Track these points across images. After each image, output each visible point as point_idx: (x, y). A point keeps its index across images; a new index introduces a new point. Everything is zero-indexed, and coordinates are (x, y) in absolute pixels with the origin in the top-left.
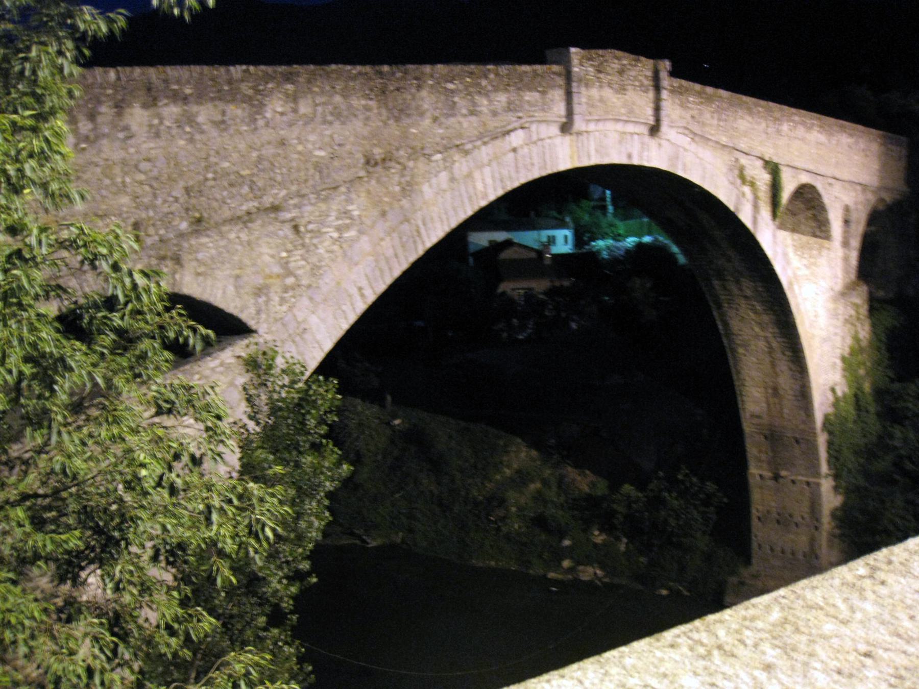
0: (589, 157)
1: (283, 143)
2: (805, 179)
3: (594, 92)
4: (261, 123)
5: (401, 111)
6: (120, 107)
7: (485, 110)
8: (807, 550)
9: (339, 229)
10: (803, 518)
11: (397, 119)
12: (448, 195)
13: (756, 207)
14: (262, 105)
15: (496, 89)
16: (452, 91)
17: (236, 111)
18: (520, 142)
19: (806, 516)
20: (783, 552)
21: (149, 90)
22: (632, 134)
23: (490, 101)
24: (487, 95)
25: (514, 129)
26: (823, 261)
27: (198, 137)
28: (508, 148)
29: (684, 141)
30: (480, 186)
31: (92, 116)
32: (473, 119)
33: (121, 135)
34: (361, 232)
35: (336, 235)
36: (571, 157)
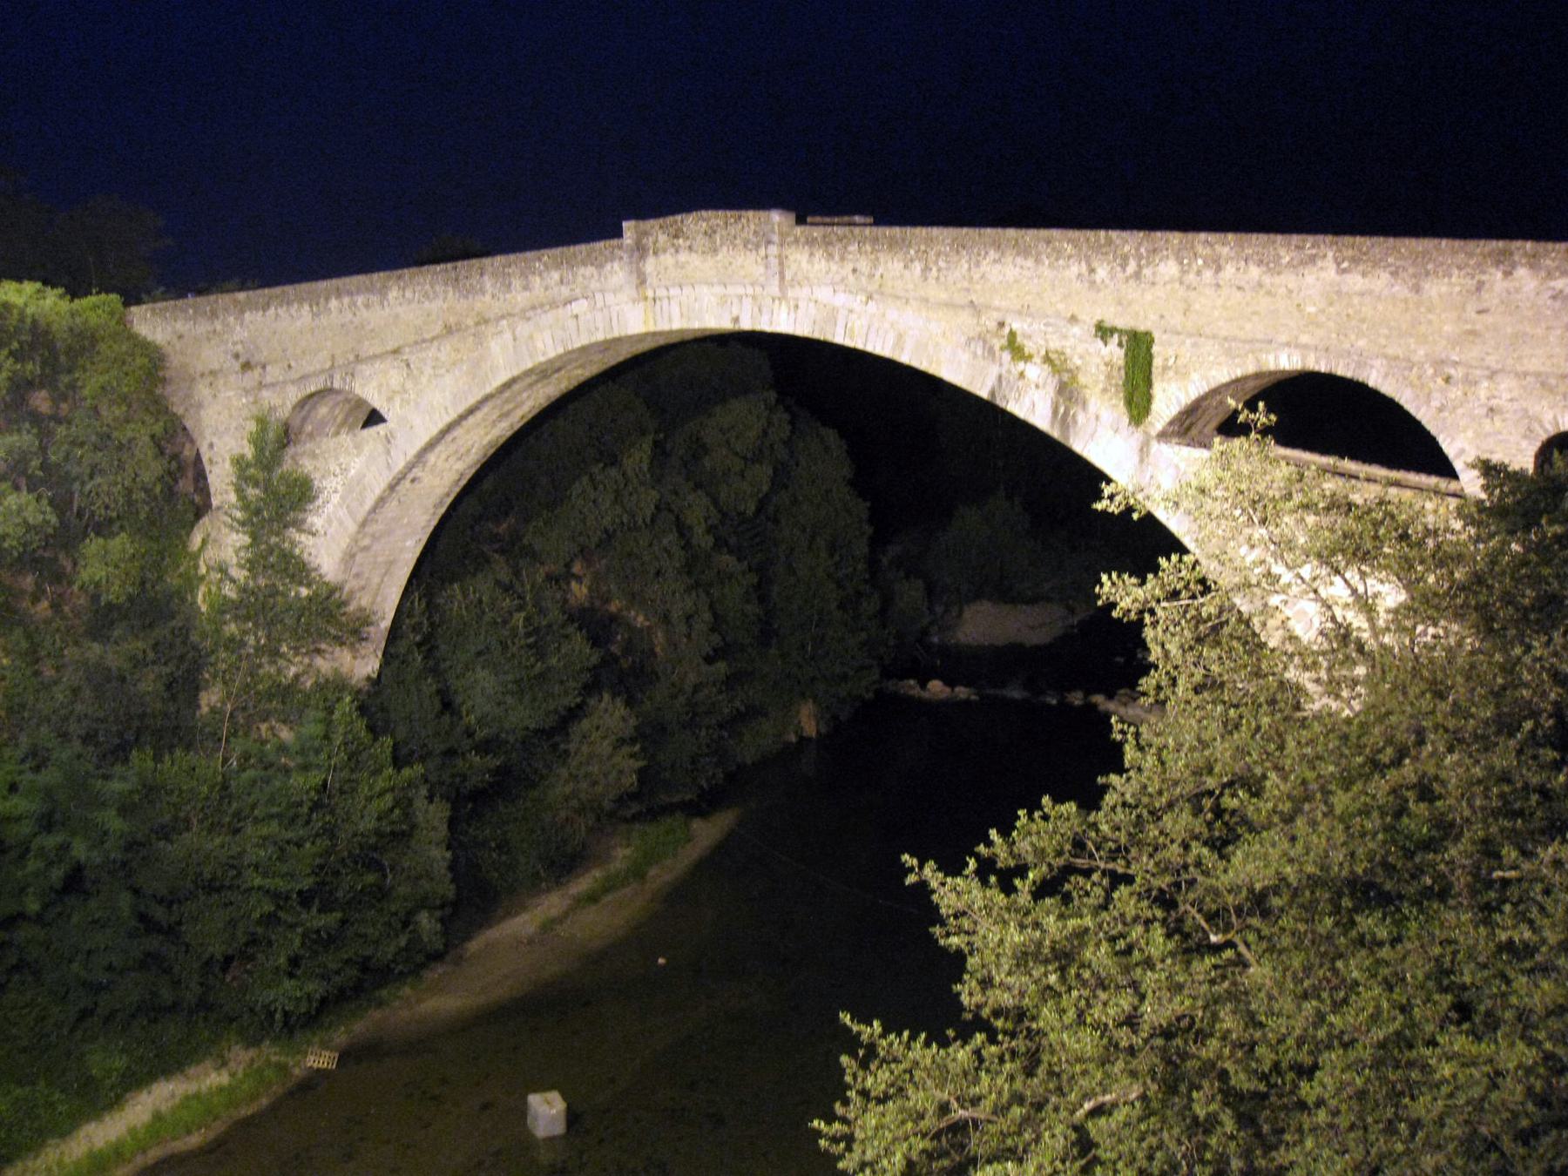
0: (670, 320)
3: (667, 259)
6: (327, 299)
9: (434, 368)
14: (386, 294)
17: (374, 298)
22: (740, 298)
24: (540, 275)
30: (540, 345)
31: (317, 304)
32: (527, 294)
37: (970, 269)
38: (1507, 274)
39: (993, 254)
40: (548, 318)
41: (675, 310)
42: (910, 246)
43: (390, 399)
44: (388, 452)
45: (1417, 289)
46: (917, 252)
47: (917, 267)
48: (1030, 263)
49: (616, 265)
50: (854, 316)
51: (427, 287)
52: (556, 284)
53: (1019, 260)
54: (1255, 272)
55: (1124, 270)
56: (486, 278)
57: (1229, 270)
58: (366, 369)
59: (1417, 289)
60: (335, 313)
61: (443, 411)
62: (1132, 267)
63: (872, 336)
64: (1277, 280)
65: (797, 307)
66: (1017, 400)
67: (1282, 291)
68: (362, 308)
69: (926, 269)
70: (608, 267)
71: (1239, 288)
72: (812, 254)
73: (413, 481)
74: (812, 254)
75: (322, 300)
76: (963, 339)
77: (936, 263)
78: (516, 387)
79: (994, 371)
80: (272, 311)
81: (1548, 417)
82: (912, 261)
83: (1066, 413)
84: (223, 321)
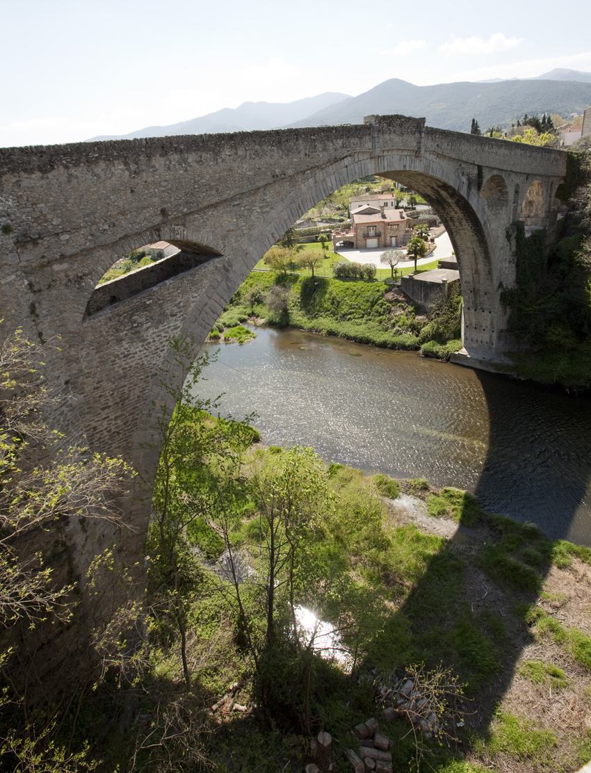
1: (230, 170)
2: (495, 172)
3: (387, 136)
4: (220, 160)
5: (289, 151)
6: (149, 157)
7: (331, 148)
8: (488, 340)
9: (261, 208)
10: (487, 327)
11: (287, 155)
12: (314, 189)
13: (469, 188)
15: (336, 138)
16: (314, 140)
17: (206, 156)
19: (489, 326)
20: (477, 341)
21: (163, 147)
23: (334, 144)
25: (346, 157)
26: (503, 212)
27: (188, 168)
28: (343, 166)
29: (432, 157)
30: (329, 184)
33: (151, 170)
34: (272, 208)
35: (259, 210)
36: (375, 169)
40: (331, 169)
47: (450, 144)
49: (367, 137)
52: (341, 148)
56: (300, 141)
60: (161, 170)
61: (270, 236)
68: (194, 164)
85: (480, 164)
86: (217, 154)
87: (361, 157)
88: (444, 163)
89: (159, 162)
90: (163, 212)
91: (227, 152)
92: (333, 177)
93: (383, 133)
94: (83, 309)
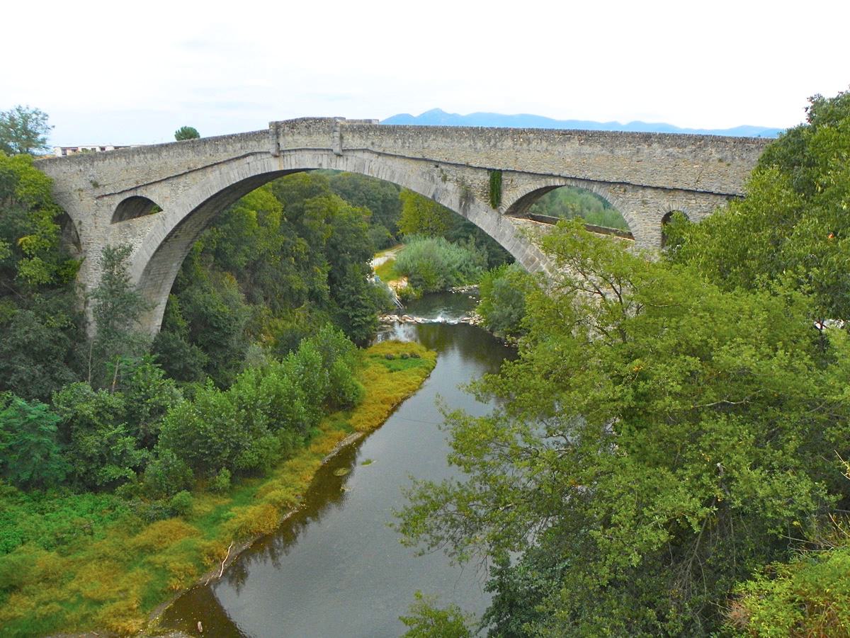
3: (289, 138)
6: (133, 156)
9: (184, 187)
17: (155, 155)
18: (252, 160)
30: (232, 176)
31: (129, 158)
34: (190, 188)
36: (280, 166)
37: (423, 143)
38: (649, 145)
39: (433, 137)
41: (293, 163)
42: (396, 133)
43: (163, 201)
44: (164, 225)
45: (612, 152)
46: (400, 135)
47: (400, 142)
48: (449, 140)
49: (266, 140)
50: (373, 163)
51: (180, 151)
53: (444, 139)
54: (545, 144)
55: (489, 143)
56: (207, 146)
57: (534, 143)
58: (153, 188)
59: (612, 152)
62: (493, 142)
63: (380, 172)
64: (555, 148)
65: (347, 159)
66: (444, 199)
67: (556, 153)
69: (404, 143)
70: (263, 141)
71: (538, 151)
72: (354, 136)
73: (176, 237)
74: (354, 136)
75: (131, 156)
76: (420, 173)
77: (408, 141)
78: (221, 195)
79: (434, 187)
80: (107, 161)
81: (666, 205)
82: (397, 139)
83: (465, 204)
84: (84, 165)
85: (488, 166)
86: (159, 155)
87: (264, 156)
88: (397, 164)
89: (136, 157)
90: (137, 182)
91: (164, 153)
92: (236, 171)
93: (284, 136)
94: (111, 218)
